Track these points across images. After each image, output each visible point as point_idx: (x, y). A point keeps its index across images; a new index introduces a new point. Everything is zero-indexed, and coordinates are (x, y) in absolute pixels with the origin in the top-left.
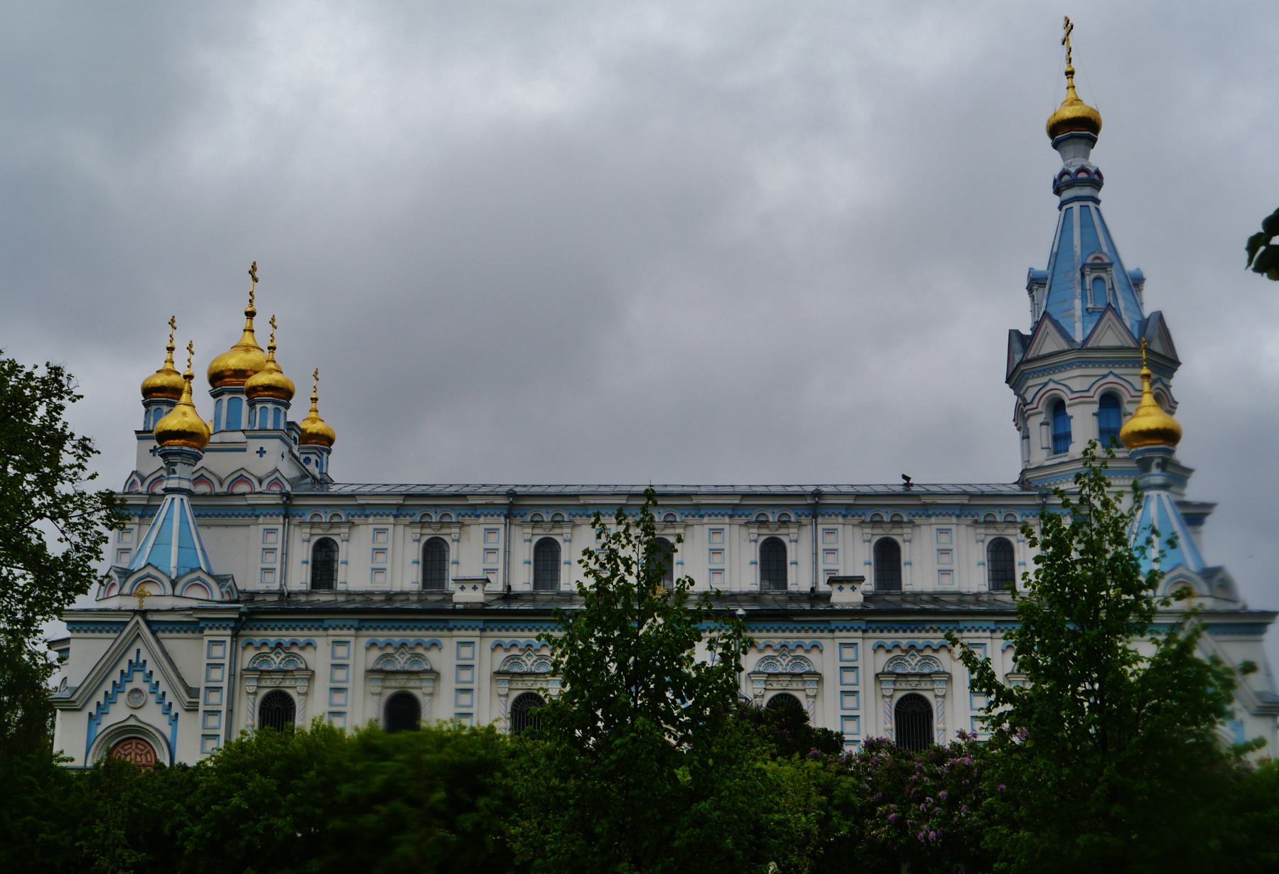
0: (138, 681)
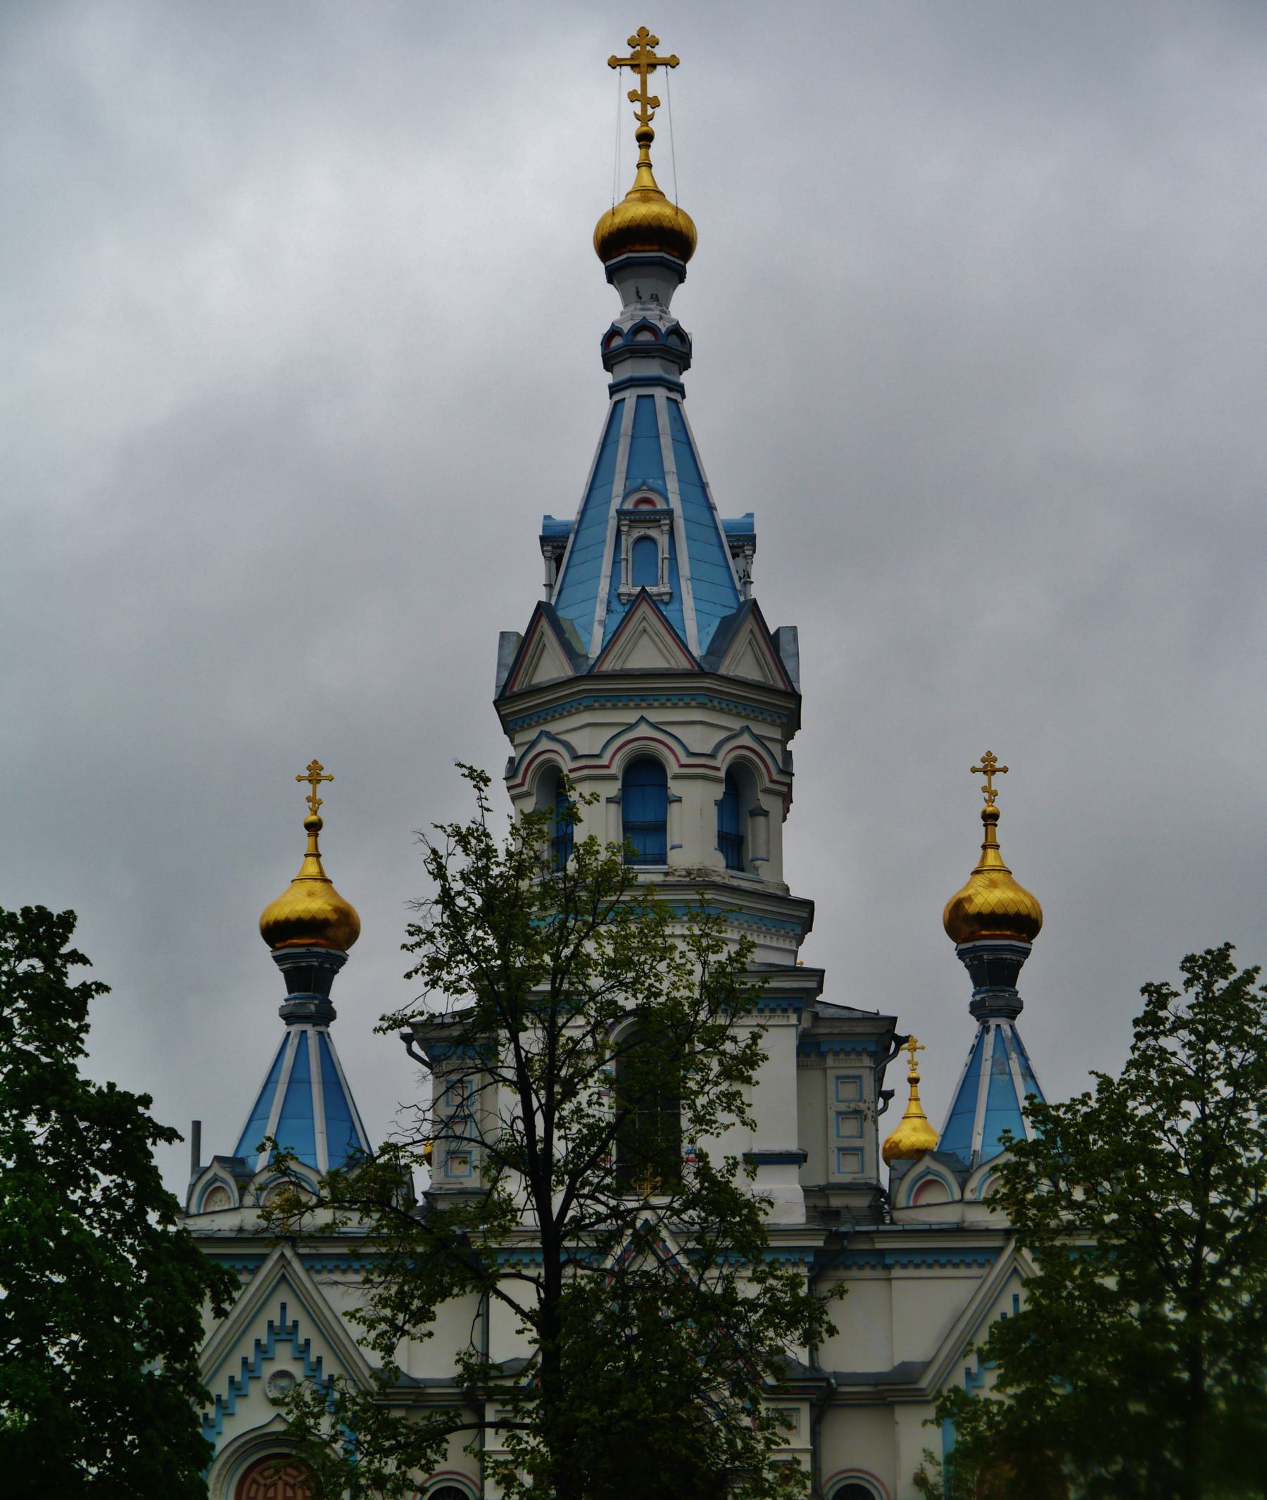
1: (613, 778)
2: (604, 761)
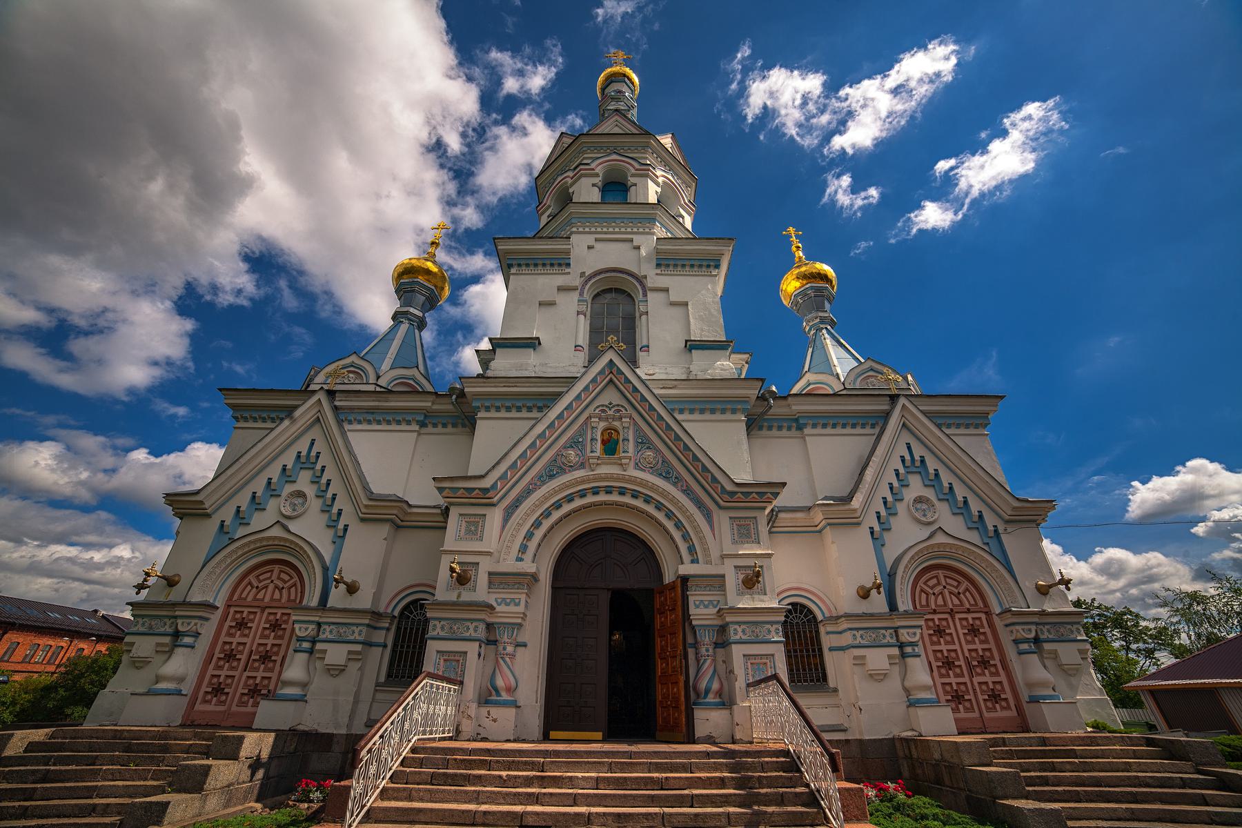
0: (303, 482)
1: (597, 175)
2: (593, 166)
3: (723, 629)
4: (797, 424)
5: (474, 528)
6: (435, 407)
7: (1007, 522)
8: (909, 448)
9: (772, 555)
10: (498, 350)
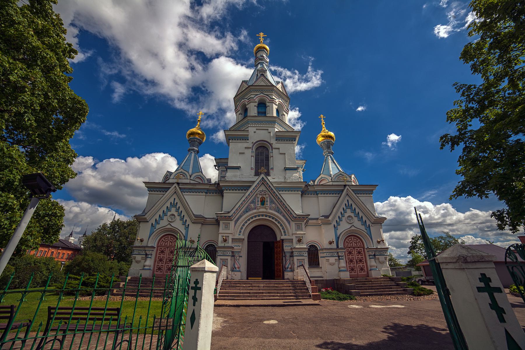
0: (173, 211)
1: (256, 102)
2: (255, 98)
3: (292, 252)
4: (316, 193)
5: (227, 227)
6: (210, 188)
7: (372, 223)
8: (348, 201)
9: (305, 234)
10: (228, 170)
